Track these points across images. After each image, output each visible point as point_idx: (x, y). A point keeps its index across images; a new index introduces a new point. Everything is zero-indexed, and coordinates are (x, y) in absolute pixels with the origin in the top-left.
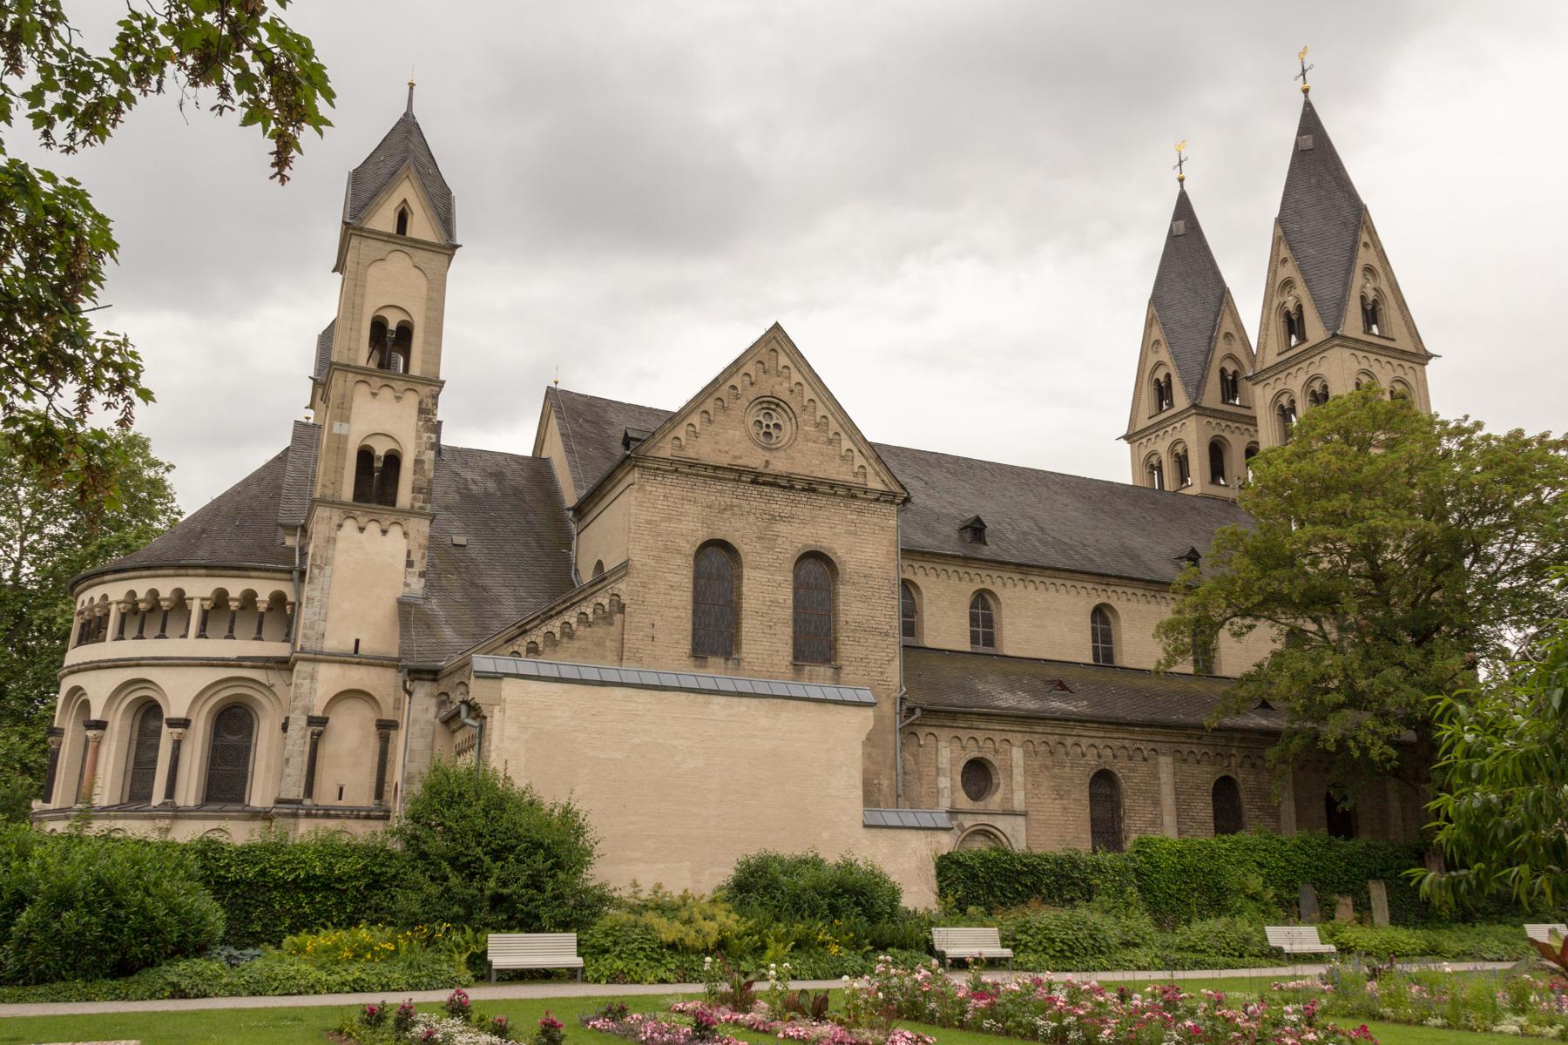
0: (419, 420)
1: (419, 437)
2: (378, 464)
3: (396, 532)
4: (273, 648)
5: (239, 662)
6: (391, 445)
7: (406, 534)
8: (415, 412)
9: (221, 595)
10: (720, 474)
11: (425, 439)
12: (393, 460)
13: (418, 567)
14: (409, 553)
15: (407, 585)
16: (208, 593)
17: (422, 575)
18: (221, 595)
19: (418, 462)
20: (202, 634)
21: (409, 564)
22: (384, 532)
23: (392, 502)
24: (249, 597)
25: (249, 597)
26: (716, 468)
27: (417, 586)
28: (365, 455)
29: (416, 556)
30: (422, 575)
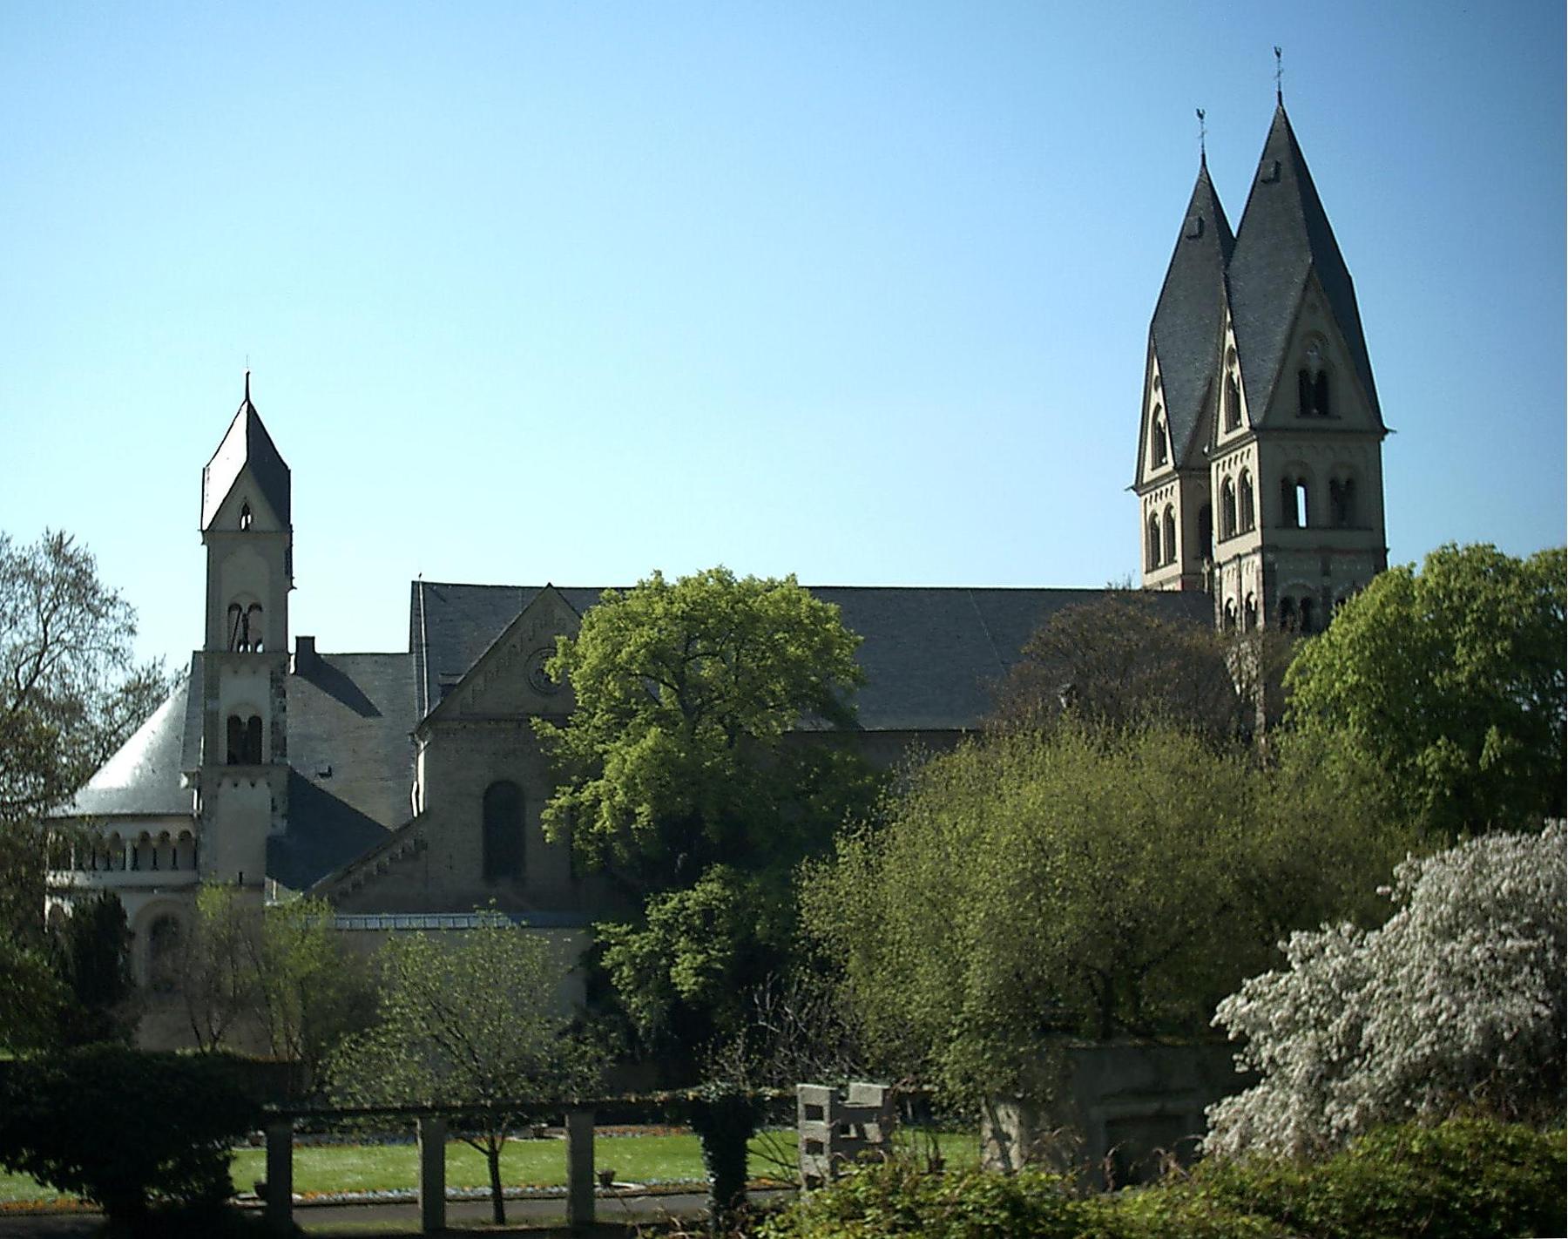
0: (272, 687)
1: (273, 703)
2: (246, 728)
3: (262, 784)
4: (181, 877)
5: (162, 888)
6: (252, 713)
7: (269, 784)
8: (268, 683)
9: (145, 837)
10: (502, 725)
11: (277, 704)
12: (256, 722)
13: (280, 811)
14: (273, 801)
15: (273, 826)
16: (136, 835)
17: (283, 816)
18: (145, 837)
19: (273, 724)
20: (135, 867)
21: (274, 809)
22: (253, 785)
23: (256, 760)
24: (165, 835)
25: (165, 835)
26: (498, 721)
27: (282, 825)
28: (234, 721)
29: (278, 802)
30: (283, 816)
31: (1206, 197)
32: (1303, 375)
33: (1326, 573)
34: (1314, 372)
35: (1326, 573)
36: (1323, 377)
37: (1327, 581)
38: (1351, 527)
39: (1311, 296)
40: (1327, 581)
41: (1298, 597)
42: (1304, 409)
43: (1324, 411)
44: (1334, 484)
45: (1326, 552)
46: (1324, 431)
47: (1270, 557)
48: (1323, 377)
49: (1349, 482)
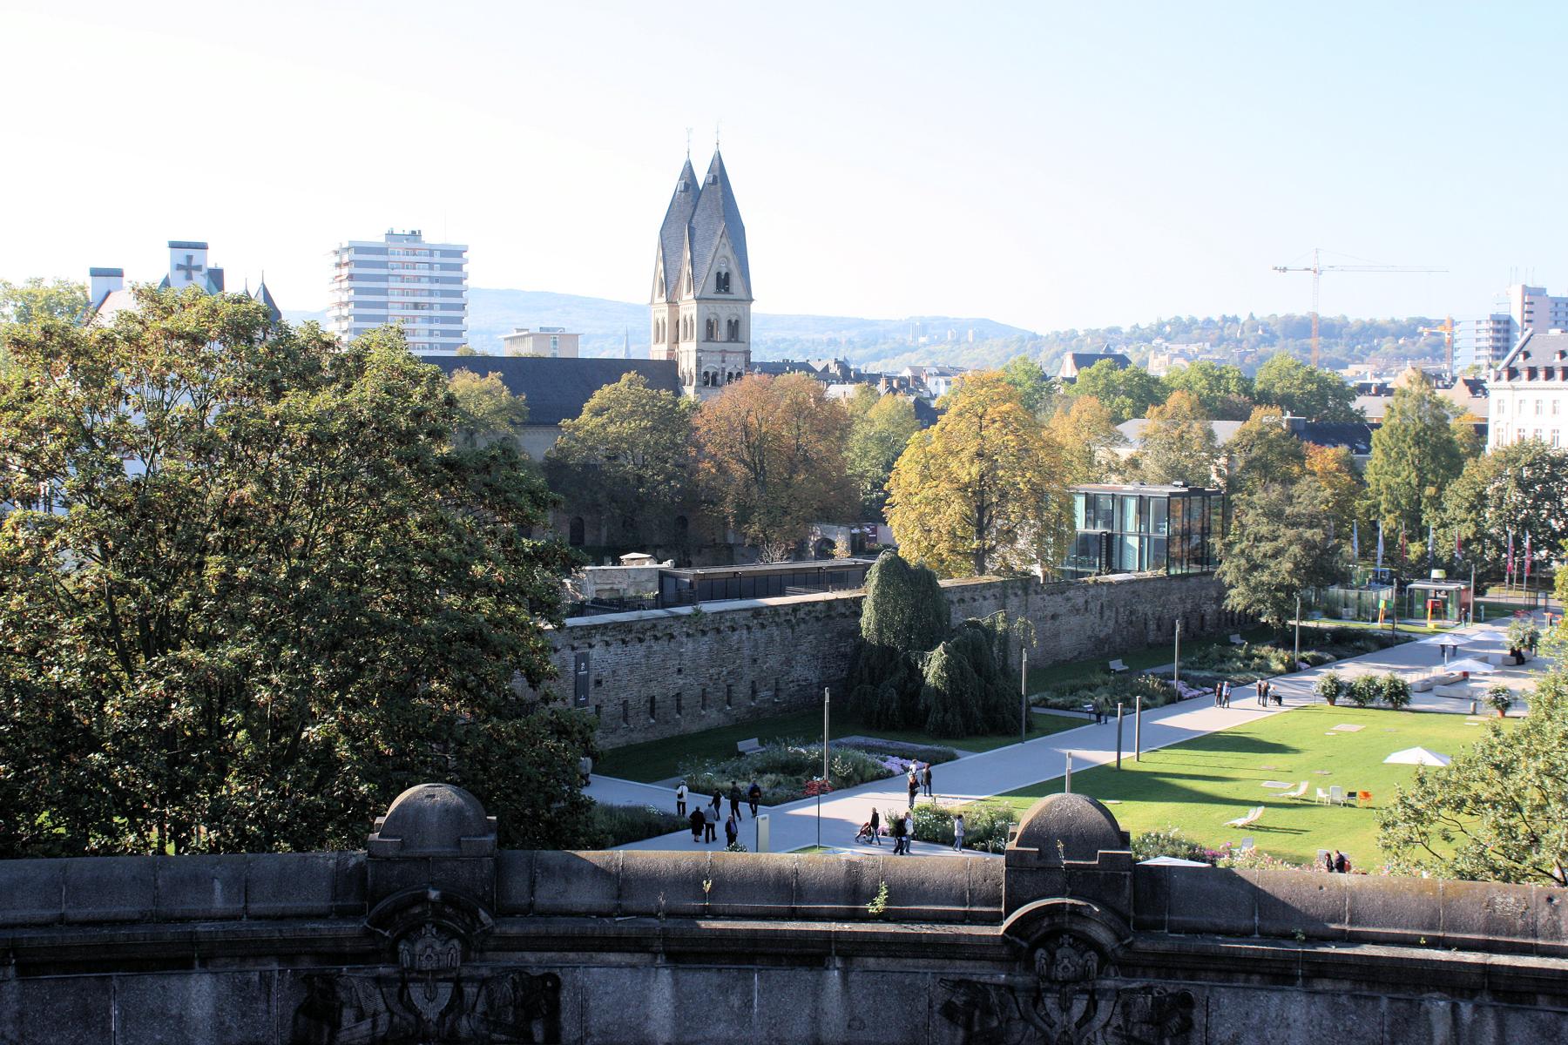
31: (689, 173)
32: (719, 274)
33: (723, 361)
34: (723, 274)
35: (723, 361)
36: (727, 274)
37: (724, 365)
38: (737, 341)
39: (724, 240)
40: (724, 365)
41: (711, 372)
42: (718, 287)
43: (727, 290)
44: (730, 322)
45: (724, 352)
46: (726, 300)
47: (700, 354)
48: (727, 275)
49: (737, 321)
